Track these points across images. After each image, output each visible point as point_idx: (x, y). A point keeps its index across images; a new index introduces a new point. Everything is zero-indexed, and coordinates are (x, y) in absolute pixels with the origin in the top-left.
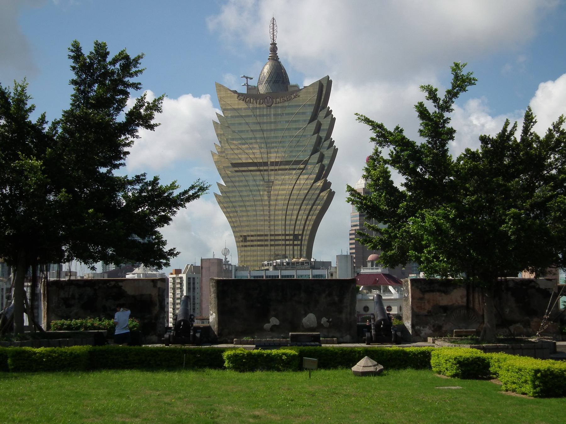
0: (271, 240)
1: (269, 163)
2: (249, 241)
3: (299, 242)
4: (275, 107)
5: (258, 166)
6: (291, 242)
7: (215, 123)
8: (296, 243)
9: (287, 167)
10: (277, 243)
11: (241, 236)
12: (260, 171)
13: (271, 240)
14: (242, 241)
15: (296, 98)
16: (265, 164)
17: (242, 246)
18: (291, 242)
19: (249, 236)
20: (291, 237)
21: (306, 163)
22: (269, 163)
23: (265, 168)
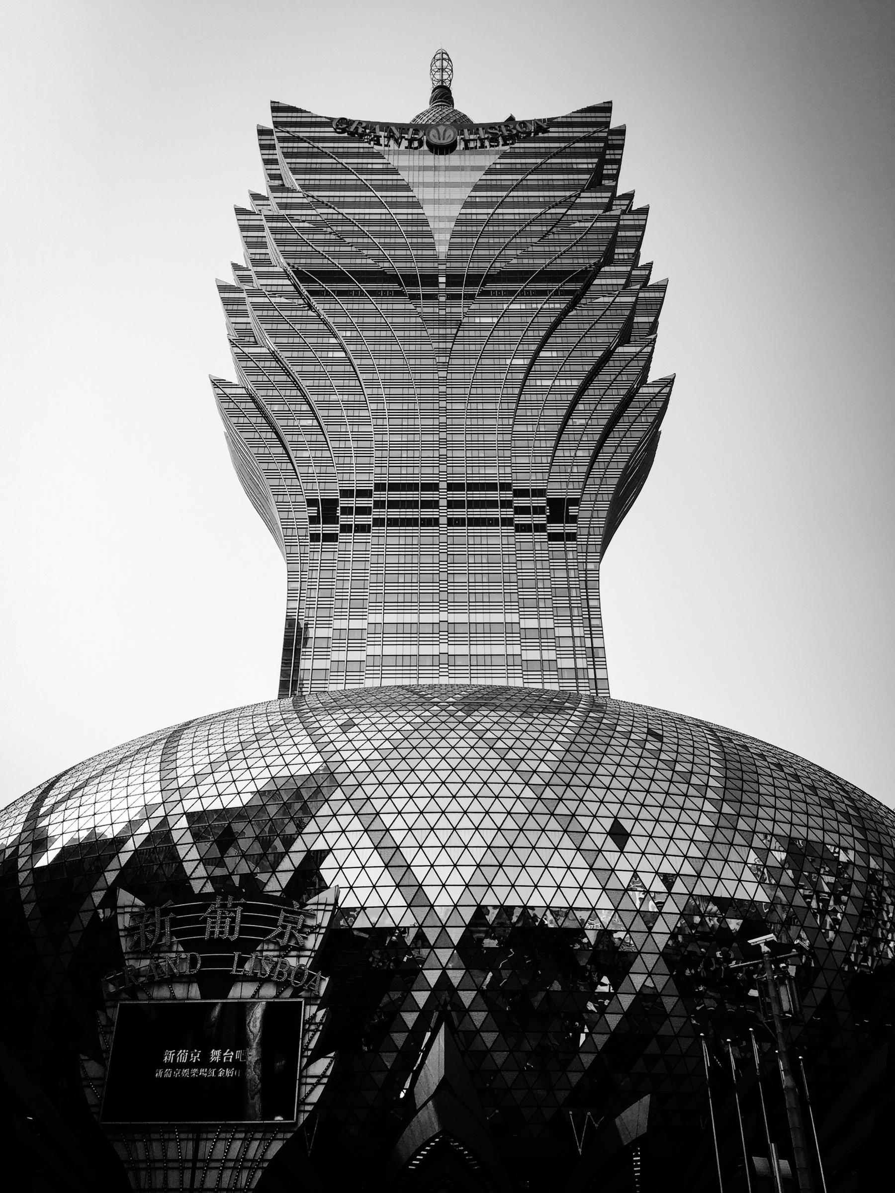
0: (451, 504)
1: (442, 280)
2: (347, 511)
3: (570, 528)
4: (460, 153)
5: (401, 285)
6: (541, 519)
7: (239, 211)
8: (556, 528)
9: (511, 286)
10: (477, 513)
11: (311, 503)
12: (413, 297)
13: (451, 504)
14: (313, 520)
15: (536, 133)
16: (430, 280)
17: (315, 538)
18: (541, 519)
19: (346, 493)
20: (541, 502)
21: (586, 277)
22: (442, 280)
23: (430, 290)
